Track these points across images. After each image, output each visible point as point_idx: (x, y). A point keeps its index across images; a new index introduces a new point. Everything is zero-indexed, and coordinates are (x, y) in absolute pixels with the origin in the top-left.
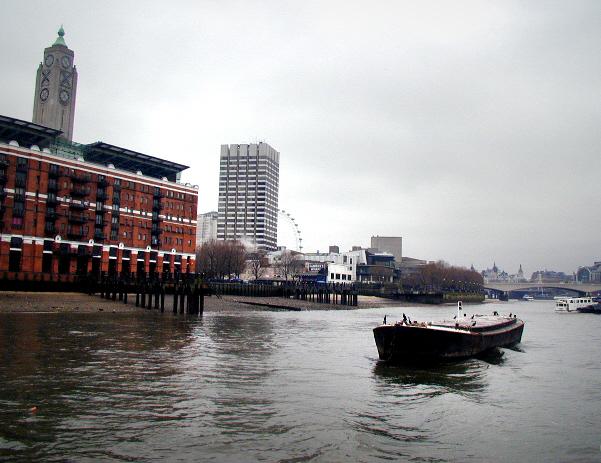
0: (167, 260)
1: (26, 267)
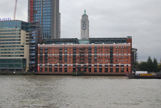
0: (96, 67)
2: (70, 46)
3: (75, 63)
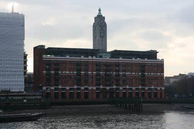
2: (92, 60)
3: (99, 85)
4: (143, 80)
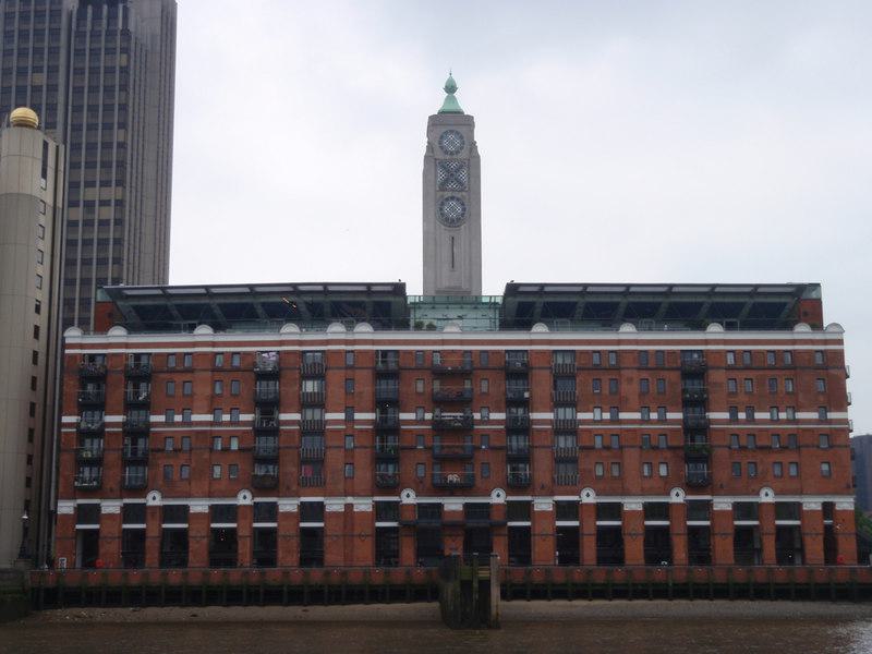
1: (333, 556)
2: (347, 342)
3: (395, 489)
4: (694, 453)
